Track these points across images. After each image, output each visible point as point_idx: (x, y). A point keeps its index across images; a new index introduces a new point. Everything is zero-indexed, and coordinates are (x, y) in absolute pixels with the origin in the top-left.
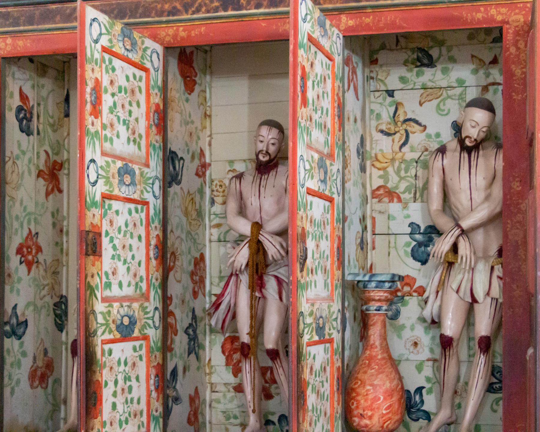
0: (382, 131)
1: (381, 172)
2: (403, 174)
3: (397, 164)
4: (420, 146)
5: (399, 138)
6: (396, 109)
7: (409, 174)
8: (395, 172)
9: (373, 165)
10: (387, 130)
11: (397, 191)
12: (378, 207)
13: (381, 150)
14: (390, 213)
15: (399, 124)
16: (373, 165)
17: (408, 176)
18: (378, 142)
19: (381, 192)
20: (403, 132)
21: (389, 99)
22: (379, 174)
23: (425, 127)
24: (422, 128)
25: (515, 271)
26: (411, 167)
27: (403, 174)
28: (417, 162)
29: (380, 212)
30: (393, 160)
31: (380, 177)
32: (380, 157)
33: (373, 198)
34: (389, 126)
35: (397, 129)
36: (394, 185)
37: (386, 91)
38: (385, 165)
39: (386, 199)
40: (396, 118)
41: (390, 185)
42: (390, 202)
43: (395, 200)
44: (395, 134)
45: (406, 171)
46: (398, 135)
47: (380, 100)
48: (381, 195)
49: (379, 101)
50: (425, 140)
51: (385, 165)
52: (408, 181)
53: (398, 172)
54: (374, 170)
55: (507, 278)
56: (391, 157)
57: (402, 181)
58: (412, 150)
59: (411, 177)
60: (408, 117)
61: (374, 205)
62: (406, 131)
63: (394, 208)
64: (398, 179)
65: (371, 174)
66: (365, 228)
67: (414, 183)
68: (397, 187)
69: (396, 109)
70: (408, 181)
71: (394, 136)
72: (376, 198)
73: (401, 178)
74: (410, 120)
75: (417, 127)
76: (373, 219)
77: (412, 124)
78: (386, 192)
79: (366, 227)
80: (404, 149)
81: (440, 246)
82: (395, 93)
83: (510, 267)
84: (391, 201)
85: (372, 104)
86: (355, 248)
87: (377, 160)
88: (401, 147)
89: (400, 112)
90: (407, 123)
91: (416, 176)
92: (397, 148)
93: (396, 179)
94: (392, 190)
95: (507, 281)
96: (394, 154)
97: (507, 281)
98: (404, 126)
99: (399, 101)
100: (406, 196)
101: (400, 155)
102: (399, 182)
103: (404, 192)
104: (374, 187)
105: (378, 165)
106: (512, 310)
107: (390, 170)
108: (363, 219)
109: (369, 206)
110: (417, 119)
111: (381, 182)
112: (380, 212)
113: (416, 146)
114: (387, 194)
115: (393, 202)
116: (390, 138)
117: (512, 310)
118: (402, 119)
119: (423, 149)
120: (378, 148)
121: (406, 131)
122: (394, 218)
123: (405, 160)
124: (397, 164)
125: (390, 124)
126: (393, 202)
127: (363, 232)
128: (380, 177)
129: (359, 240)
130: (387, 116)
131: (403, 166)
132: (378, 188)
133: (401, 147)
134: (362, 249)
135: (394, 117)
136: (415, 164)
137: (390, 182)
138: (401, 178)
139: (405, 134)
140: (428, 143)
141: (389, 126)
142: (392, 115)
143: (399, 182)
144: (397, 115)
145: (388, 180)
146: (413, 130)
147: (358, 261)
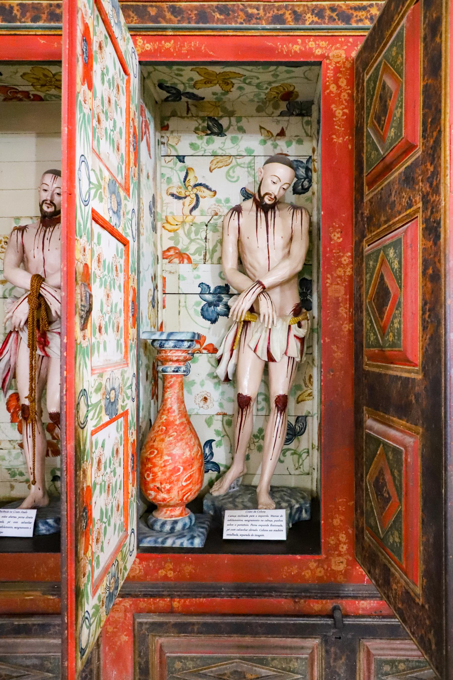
0: (173, 195)
1: (172, 234)
2: (193, 236)
3: (187, 227)
4: (210, 211)
5: (189, 202)
6: (187, 173)
7: (199, 237)
8: (185, 234)
9: (163, 227)
10: (177, 194)
11: (187, 253)
12: (169, 267)
13: (172, 213)
14: (181, 274)
15: (190, 188)
16: (163, 227)
17: (198, 239)
18: (169, 205)
19: (172, 252)
20: (193, 196)
21: (180, 164)
22: (169, 236)
23: (215, 192)
24: (212, 193)
25: (335, 331)
26: (201, 230)
27: (193, 236)
28: (207, 226)
29: (170, 272)
30: (183, 222)
31: (171, 238)
32: (170, 219)
33: (164, 258)
34: (180, 190)
35: (187, 193)
36: (185, 247)
37: (176, 156)
38: (176, 227)
39: (176, 260)
40: (186, 182)
41: (180, 247)
42: (180, 263)
43: (186, 261)
44: (185, 198)
45: (197, 233)
46: (188, 199)
47: (171, 164)
48: (172, 255)
49: (170, 166)
50: (215, 204)
51: (176, 227)
52: (198, 243)
53: (188, 234)
54: (165, 232)
55: (326, 339)
56: (181, 220)
57: (193, 243)
58: (202, 214)
59: (202, 240)
60: (199, 182)
61: (164, 265)
62: (197, 196)
63: (185, 268)
64: (189, 241)
65: (161, 235)
66: (156, 287)
67: (204, 245)
68: (187, 249)
69: (187, 173)
70: (198, 243)
71: (184, 200)
72: (166, 258)
73: (192, 241)
74: (200, 185)
75: (207, 192)
76: (164, 279)
77: (202, 189)
78: (177, 253)
79: (157, 287)
80: (194, 213)
81: (240, 303)
82: (186, 158)
83: (330, 326)
84: (181, 261)
85: (163, 168)
86: (148, 305)
87: (167, 222)
88: (191, 211)
89: (190, 177)
90: (197, 187)
91: (206, 238)
92: (187, 211)
93: (187, 241)
94: (183, 252)
95: (327, 341)
96: (185, 217)
97: (327, 341)
98: (195, 190)
99: (190, 166)
100: (196, 258)
101: (190, 218)
102: (190, 243)
103: (194, 254)
104: (165, 248)
105: (168, 226)
106: (332, 374)
107: (181, 232)
108: (154, 278)
109: (159, 266)
110: (207, 184)
111: (171, 244)
112: (170, 272)
113: (206, 210)
114: (177, 255)
115: (183, 263)
116: (181, 201)
117: (332, 374)
118: (192, 183)
119: (213, 213)
120: (169, 211)
121: (197, 196)
122: (184, 279)
123: (195, 223)
124: (187, 227)
125: (180, 188)
126: (183, 263)
127: (154, 290)
128: (171, 238)
129: (151, 298)
130: (178, 180)
131: (193, 228)
132: (169, 250)
133: (191, 211)
134: (153, 307)
135: (184, 182)
136: (205, 227)
137: (181, 243)
138: (192, 241)
139: (195, 198)
140: (218, 207)
141: (180, 190)
142: (182, 180)
143: (190, 243)
144: (188, 179)
145: (179, 242)
146: (204, 195)
147: (149, 319)
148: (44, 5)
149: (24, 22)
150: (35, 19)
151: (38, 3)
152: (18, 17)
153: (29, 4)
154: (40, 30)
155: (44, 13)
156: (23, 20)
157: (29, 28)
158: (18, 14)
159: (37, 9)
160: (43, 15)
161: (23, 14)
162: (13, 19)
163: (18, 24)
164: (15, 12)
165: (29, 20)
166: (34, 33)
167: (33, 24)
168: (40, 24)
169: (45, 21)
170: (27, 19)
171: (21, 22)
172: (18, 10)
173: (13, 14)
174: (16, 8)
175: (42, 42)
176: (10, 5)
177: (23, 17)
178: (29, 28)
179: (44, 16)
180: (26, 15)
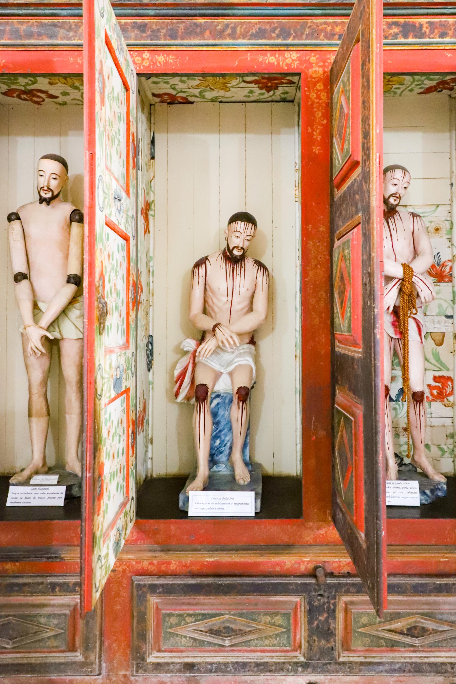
148: (450, 23)
149: (433, 38)
150: (442, 35)
151: (445, 21)
152: (427, 33)
153: (437, 22)
154: (450, 45)
155: (451, 30)
156: (432, 36)
157: (440, 44)
158: (428, 31)
159: (444, 26)
160: (449, 32)
161: (432, 32)
162: (423, 35)
163: (427, 40)
164: (424, 29)
165: (437, 36)
166: (443, 48)
167: (440, 40)
168: (447, 40)
169: (451, 37)
170: (436, 35)
171: (429, 38)
172: (427, 28)
173: (423, 31)
174: (425, 26)
175: (449, 55)
176: (420, 23)
177: (432, 33)
178: (440, 44)
179: (451, 33)
180: (434, 32)
